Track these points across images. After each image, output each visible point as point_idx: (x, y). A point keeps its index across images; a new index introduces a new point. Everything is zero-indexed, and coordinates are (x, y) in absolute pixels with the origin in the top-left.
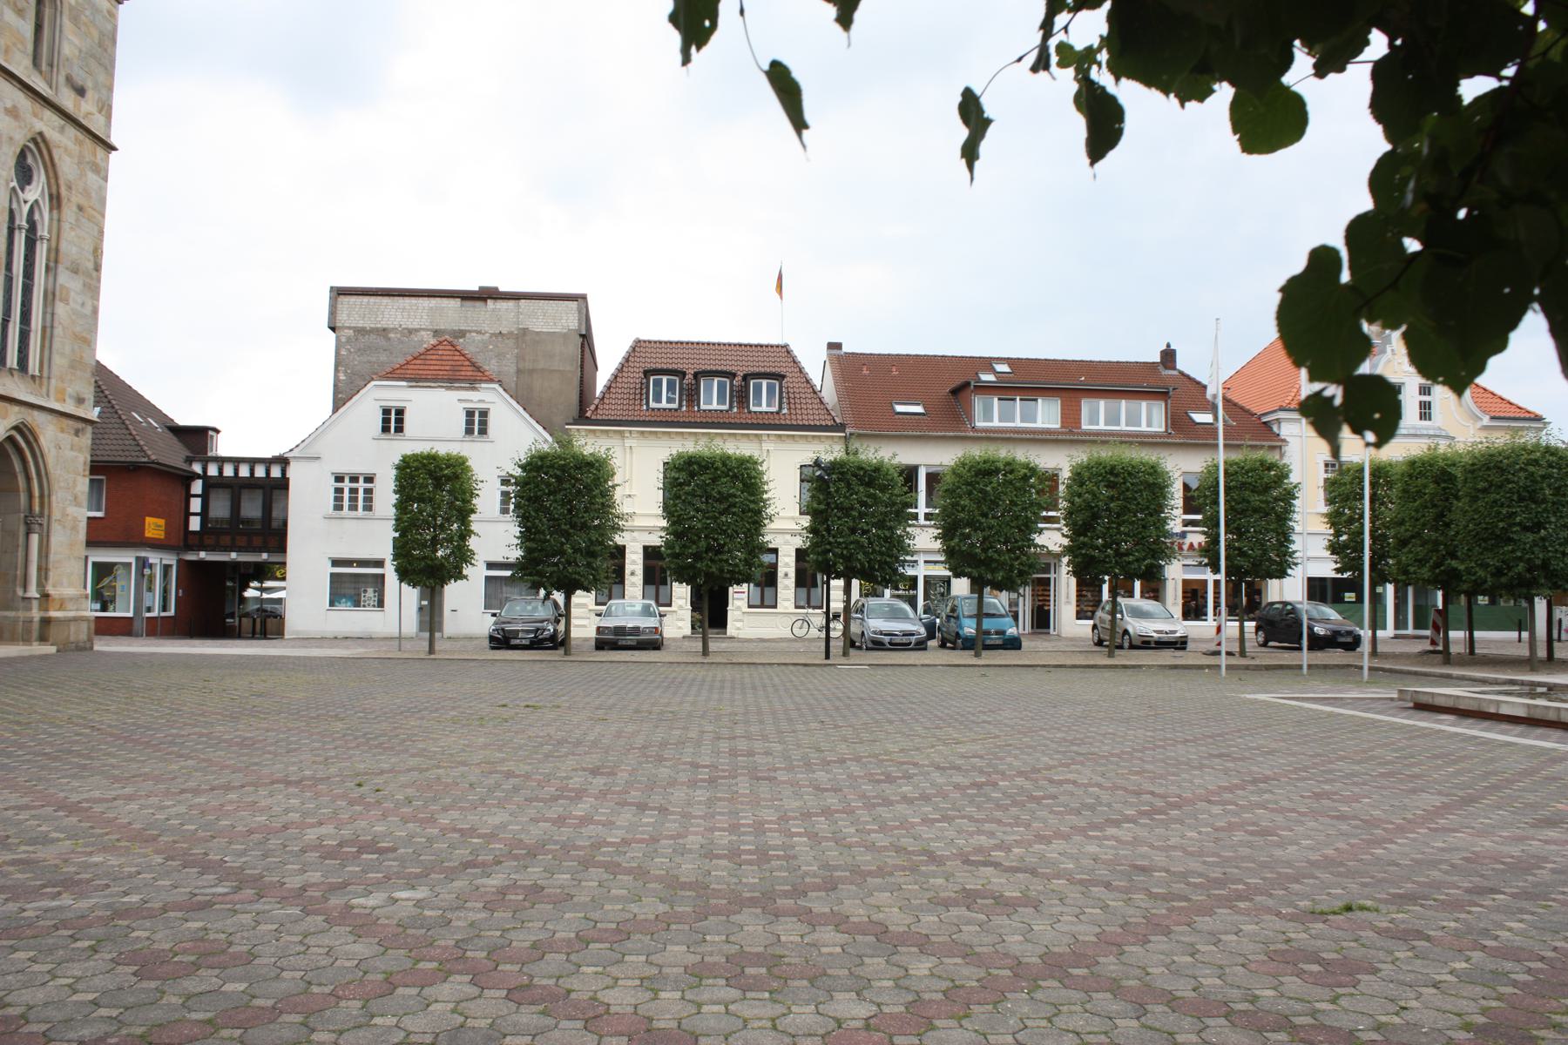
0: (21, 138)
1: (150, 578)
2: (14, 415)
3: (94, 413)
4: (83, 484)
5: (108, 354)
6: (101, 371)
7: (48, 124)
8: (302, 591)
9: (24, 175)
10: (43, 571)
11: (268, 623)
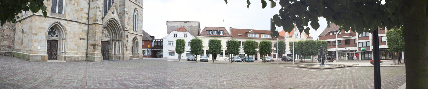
0: (134, 8)
1: (148, 51)
2: (135, 35)
3: (142, 35)
4: (142, 42)
5: (144, 29)
6: (143, 31)
7: (137, 7)
8: (165, 52)
9: (135, 12)
10: (138, 51)
11: (161, 56)
